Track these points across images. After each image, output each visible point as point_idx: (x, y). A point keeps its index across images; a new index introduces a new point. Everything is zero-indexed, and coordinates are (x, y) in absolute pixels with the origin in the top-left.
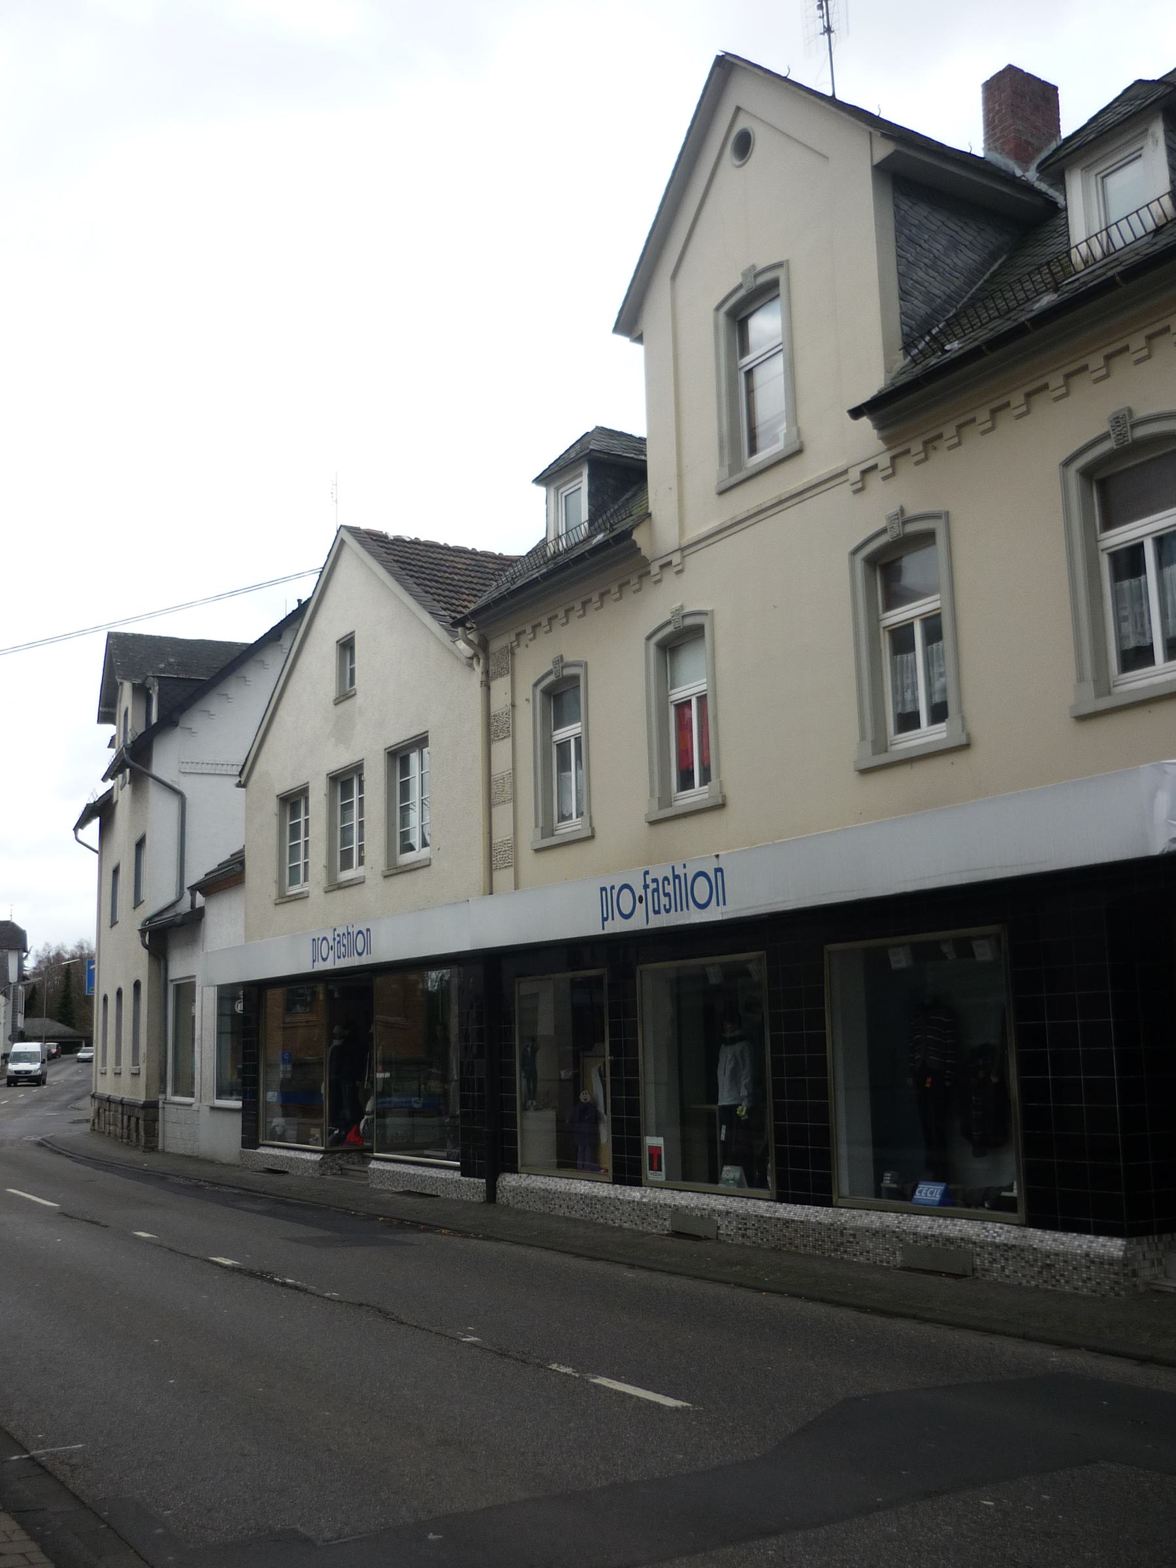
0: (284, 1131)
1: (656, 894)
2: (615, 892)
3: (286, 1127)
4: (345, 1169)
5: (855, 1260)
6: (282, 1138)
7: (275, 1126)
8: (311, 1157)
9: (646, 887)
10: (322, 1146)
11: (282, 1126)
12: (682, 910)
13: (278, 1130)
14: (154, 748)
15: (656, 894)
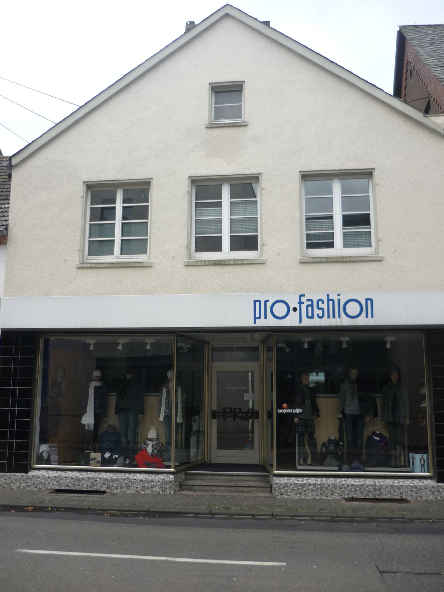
0: (49, 456)
1: (310, 308)
2: (269, 305)
3: (50, 452)
4: (185, 485)
5: (128, 492)
6: (48, 461)
7: (42, 452)
8: (375, 482)
9: (300, 303)
10: (428, 472)
11: (47, 452)
12: (334, 317)
13: (45, 455)
14: (13, 171)
15: (310, 308)
